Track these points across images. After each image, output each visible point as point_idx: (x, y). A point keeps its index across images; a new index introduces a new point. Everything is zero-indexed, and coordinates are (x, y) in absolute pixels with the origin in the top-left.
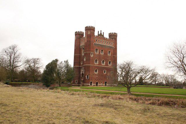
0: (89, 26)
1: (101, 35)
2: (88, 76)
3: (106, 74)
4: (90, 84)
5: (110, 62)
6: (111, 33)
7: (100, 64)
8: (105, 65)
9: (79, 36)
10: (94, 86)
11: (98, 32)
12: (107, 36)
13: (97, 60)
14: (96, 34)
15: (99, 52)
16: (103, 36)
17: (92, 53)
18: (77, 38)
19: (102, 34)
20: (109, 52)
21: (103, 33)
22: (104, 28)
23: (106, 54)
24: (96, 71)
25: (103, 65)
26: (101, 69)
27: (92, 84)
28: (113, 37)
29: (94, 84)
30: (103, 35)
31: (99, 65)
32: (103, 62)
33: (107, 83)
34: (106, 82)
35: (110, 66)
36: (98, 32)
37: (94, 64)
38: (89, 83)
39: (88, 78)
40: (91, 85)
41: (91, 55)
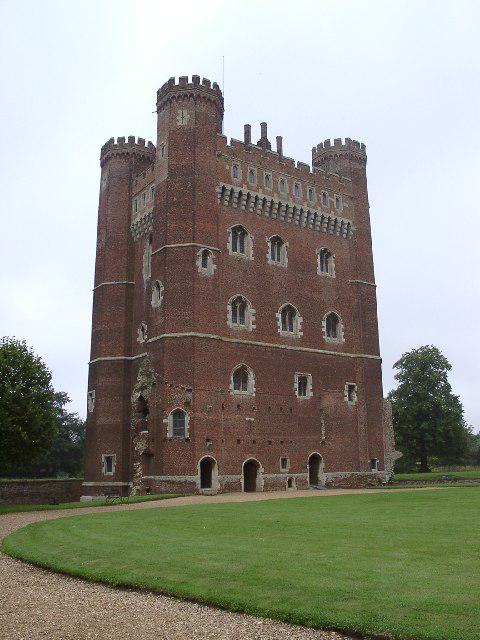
0: (183, 80)
2: (179, 415)
4: (197, 479)
5: (332, 322)
6: (327, 142)
7: (265, 328)
8: (303, 341)
9: (120, 165)
10: (228, 488)
11: (248, 128)
13: (244, 306)
14: (232, 130)
15: (260, 253)
17: (206, 254)
18: (110, 177)
19: (274, 148)
20: (325, 254)
21: (279, 139)
22: (281, 109)
24: (241, 378)
25: (287, 340)
26: (276, 367)
27: (215, 473)
28: (343, 164)
29: (234, 478)
30: (280, 150)
31: (259, 333)
32: (288, 324)
33: (322, 465)
34: (315, 460)
35: (335, 348)
36: (248, 128)
37: (226, 331)
38: (193, 472)
39: (178, 431)
40: (206, 481)
41: (199, 263)
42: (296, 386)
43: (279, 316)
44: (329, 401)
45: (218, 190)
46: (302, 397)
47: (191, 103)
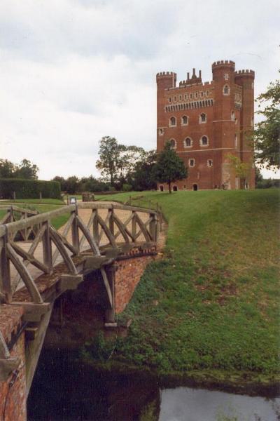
1: (195, 81)
3: (196, 169)
8: (192, 149)
11: (188, 74)
12: (207, 77)
16: (200, 80)
23: (194, 122)
25: (188, 149)
36: (188, 74)
42: (189, 163)
43: (185, 142)
44: (201, 167)
45: (165, 108)
46: (190, 166)
47: (164, 81)
